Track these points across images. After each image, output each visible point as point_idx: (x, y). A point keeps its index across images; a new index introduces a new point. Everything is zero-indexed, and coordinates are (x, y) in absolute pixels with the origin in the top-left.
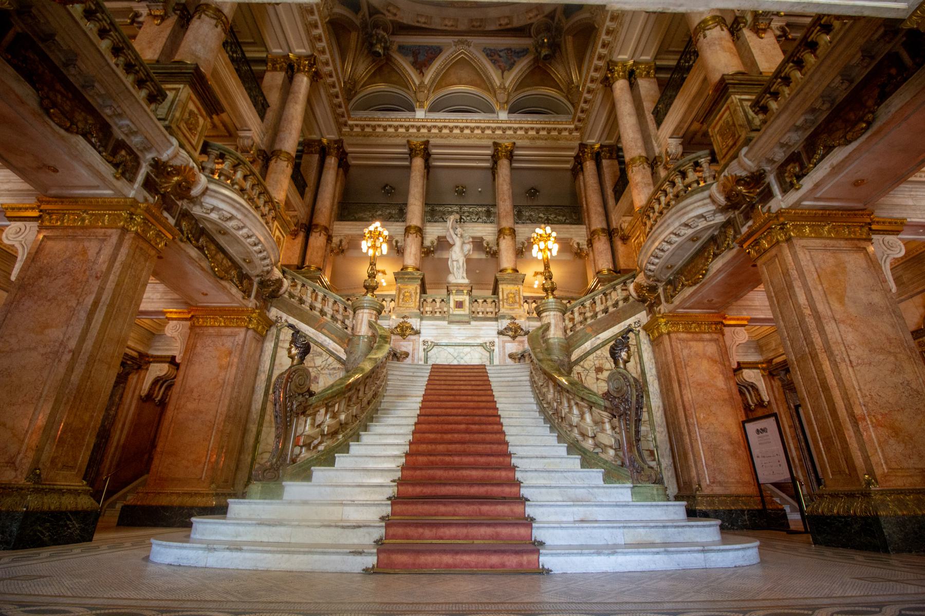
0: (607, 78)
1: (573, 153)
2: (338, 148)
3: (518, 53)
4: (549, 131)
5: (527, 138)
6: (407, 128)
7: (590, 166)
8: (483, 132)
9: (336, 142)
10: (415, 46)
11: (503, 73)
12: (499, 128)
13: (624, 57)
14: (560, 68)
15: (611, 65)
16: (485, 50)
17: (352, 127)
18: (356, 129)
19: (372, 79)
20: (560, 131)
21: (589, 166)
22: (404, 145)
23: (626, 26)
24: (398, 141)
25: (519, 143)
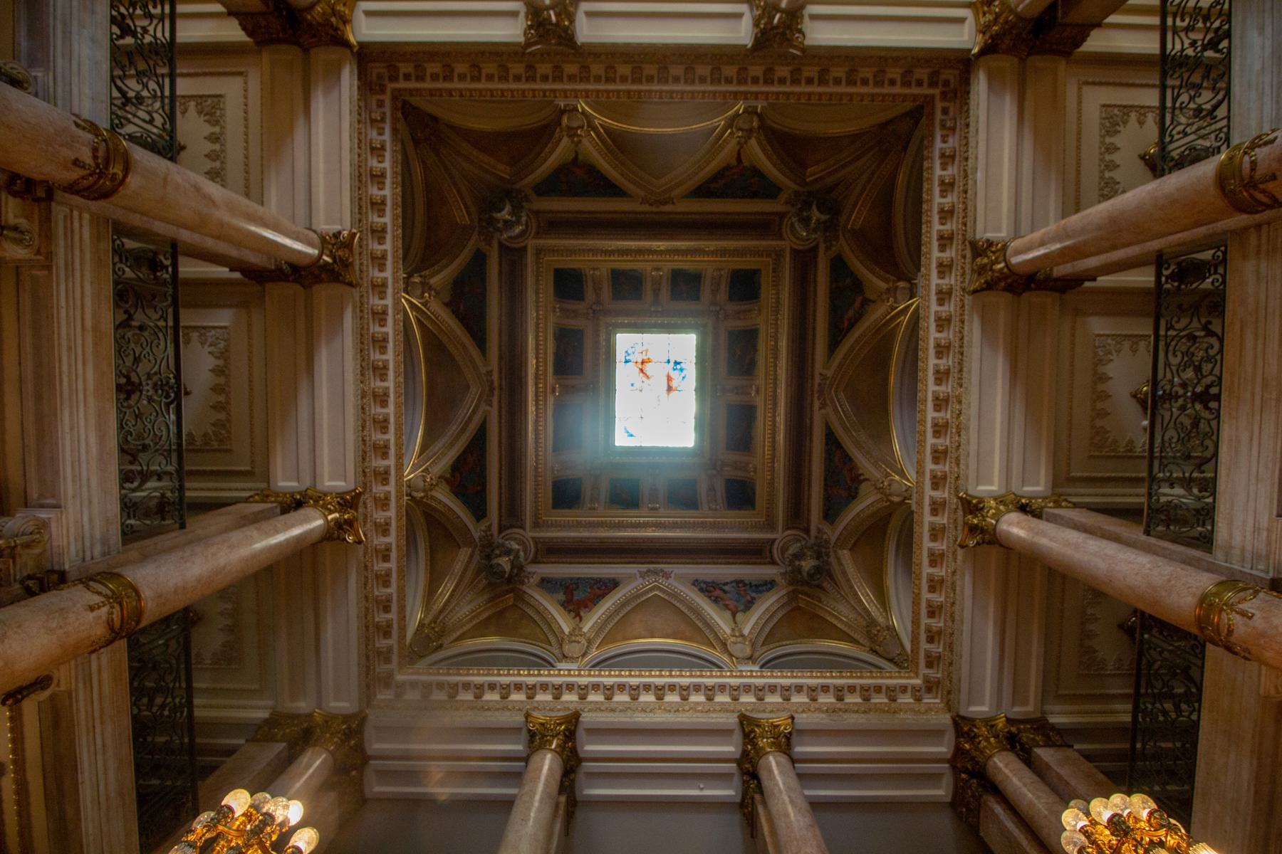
0: (973, 529)
1: (943, 748)
2: (349, 734)
4: (866, 692)
5: (819, 710)
6: (531, 691)
7: (1006, 767)
8: (710, 699)
9: (346, 718)
10: (571, 579)
11: (734, 615)
12: (747, 688)
13: (988, 487)
14: (842, 608)
15: (972, 506)
16: (696, 583)
17: (401, 686)
18: (412, 696)
19: (482, 628)
20: (892, 693)
21: (1006, 767)
22: (519, 730)
23: (973, 425)
25: (803, 719)
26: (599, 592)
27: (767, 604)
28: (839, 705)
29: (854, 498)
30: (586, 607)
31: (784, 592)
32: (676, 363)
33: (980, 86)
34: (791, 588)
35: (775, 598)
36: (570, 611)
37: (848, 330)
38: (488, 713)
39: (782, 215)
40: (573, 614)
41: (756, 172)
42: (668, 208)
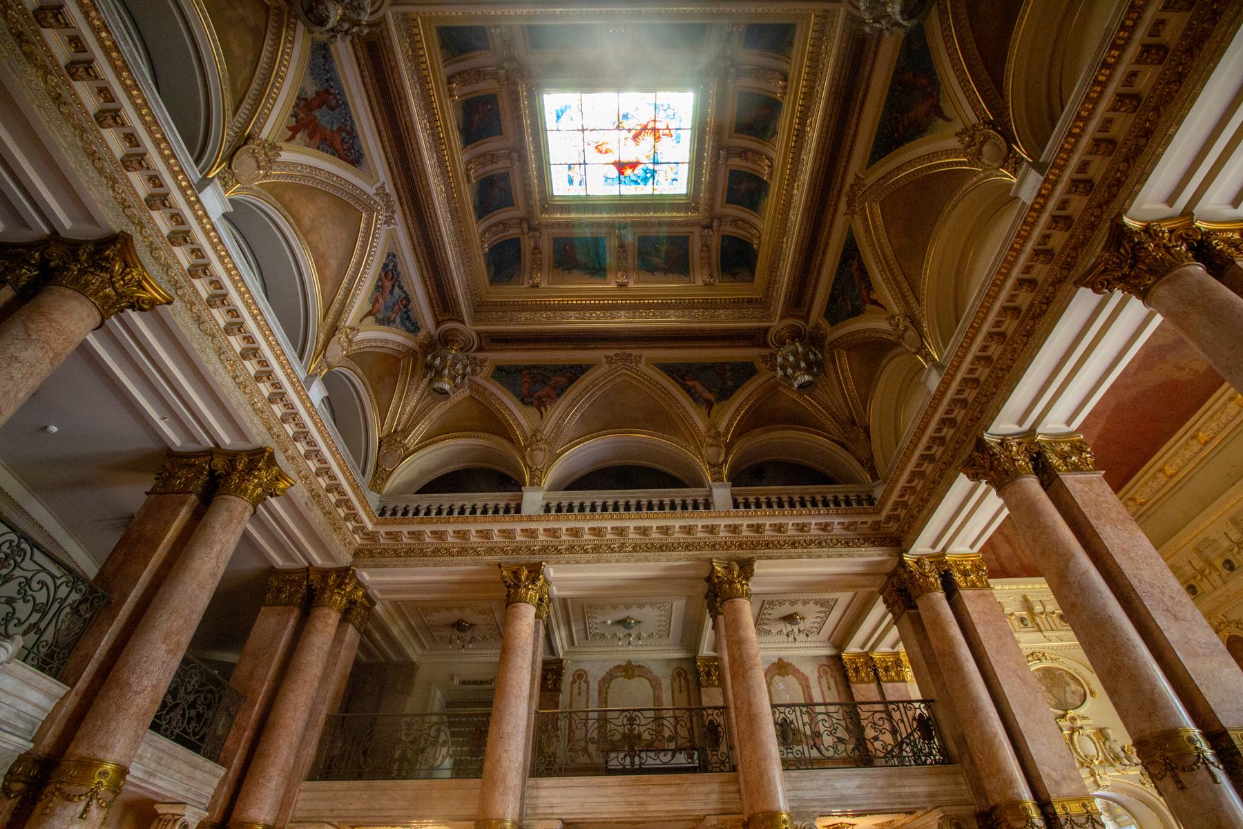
0: (516, 574)
3: (408, 318)
10: (342, 93)
11: (370, 313)
13: (551, 572)
16: (391, 256)
20: (353, 516)
24: (97, 196)
26: (337, 142)
27: (392, 337)
28: (321, 492)
29: (523, 401)
30: (311, 136)
31: (410, 344)
32: (654, 171)
33: (873, 556)
34: (417, 348)
35: (400, 339)
36: (295, 115)
37: (682, 385)
38: (87, 162)
39: (806, 318)
40: (293, 122)
41: (857, 312)
42: (843, 206)
